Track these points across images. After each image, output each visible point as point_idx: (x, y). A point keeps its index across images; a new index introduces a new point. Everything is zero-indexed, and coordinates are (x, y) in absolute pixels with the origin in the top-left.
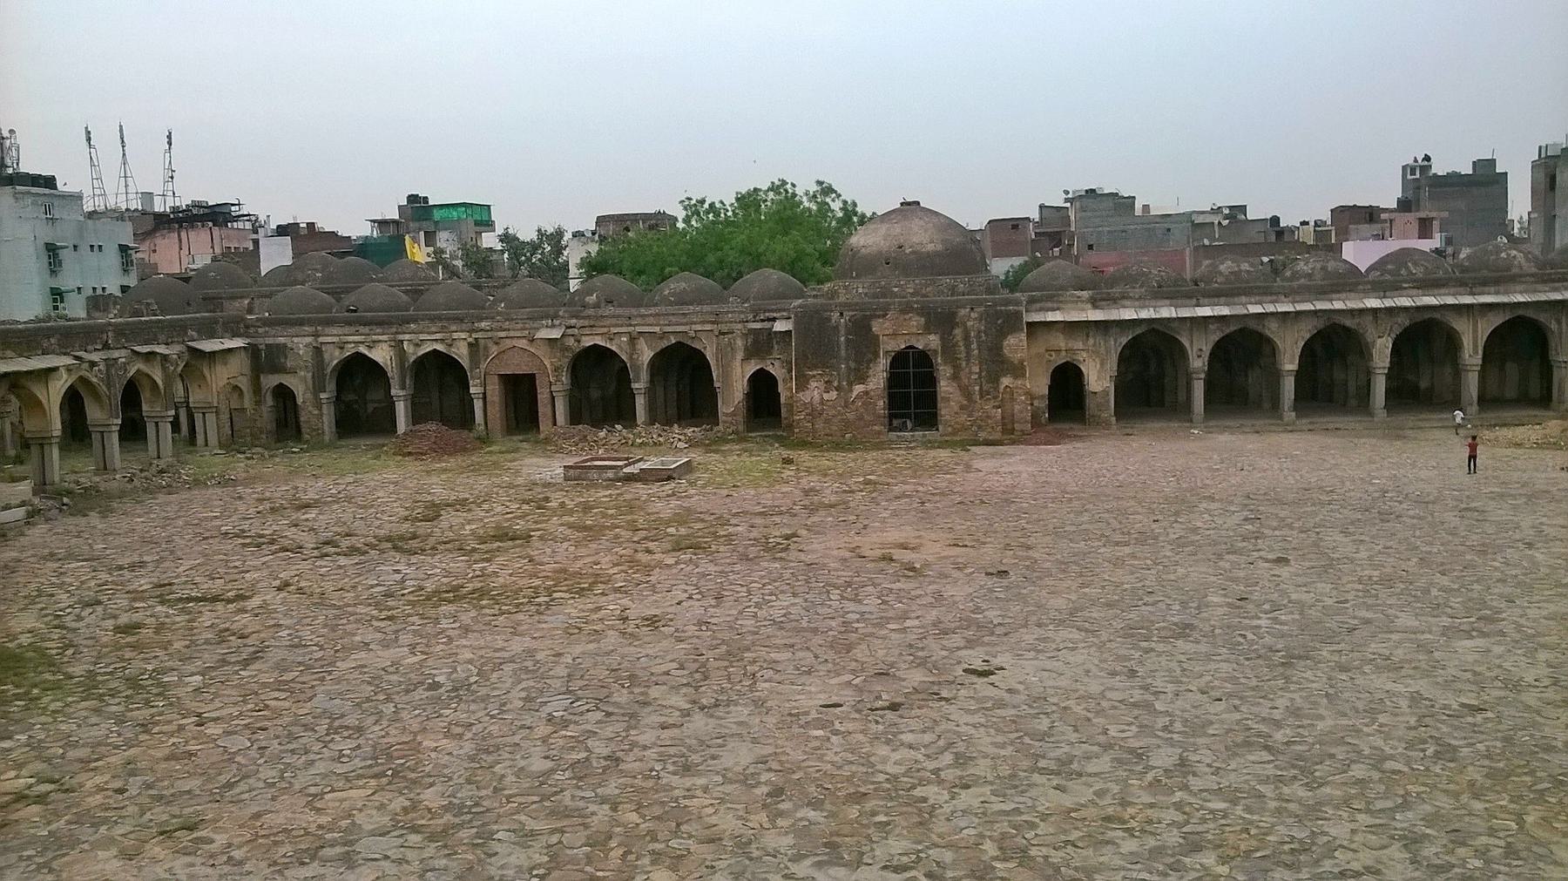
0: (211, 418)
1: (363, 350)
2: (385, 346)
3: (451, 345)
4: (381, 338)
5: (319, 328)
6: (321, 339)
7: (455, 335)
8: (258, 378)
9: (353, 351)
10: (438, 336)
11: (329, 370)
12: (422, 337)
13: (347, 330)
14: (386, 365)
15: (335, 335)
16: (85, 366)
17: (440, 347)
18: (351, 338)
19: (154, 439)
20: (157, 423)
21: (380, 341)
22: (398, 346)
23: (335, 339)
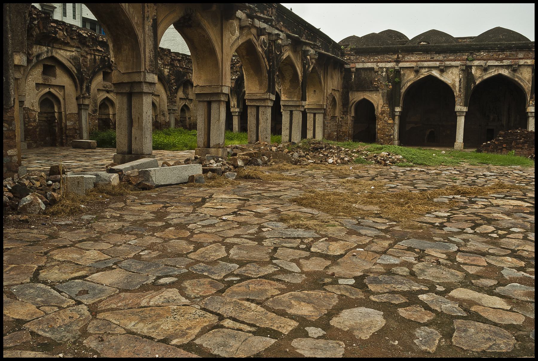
0: (319, 118)
1: (436, 73)
2: (456, 71)
3: (515, 71)
4: (453, 63)
5: (400, 56)
6: (401, 65)
7: (522, 62)
8: (347, 93)
9: (426, 74)
10: (506, 62)
11: (403, 90)
12: (490, 63)
13: (422, 58)
14: (454, 85)
15: (412, 61)
16: (254, 31)
17: (505, 72)
18: (426, 64)
19: (288, 125)
20: (291, 112)
21: (452, 67)
22: (467, 71)
23: (413, 65)
